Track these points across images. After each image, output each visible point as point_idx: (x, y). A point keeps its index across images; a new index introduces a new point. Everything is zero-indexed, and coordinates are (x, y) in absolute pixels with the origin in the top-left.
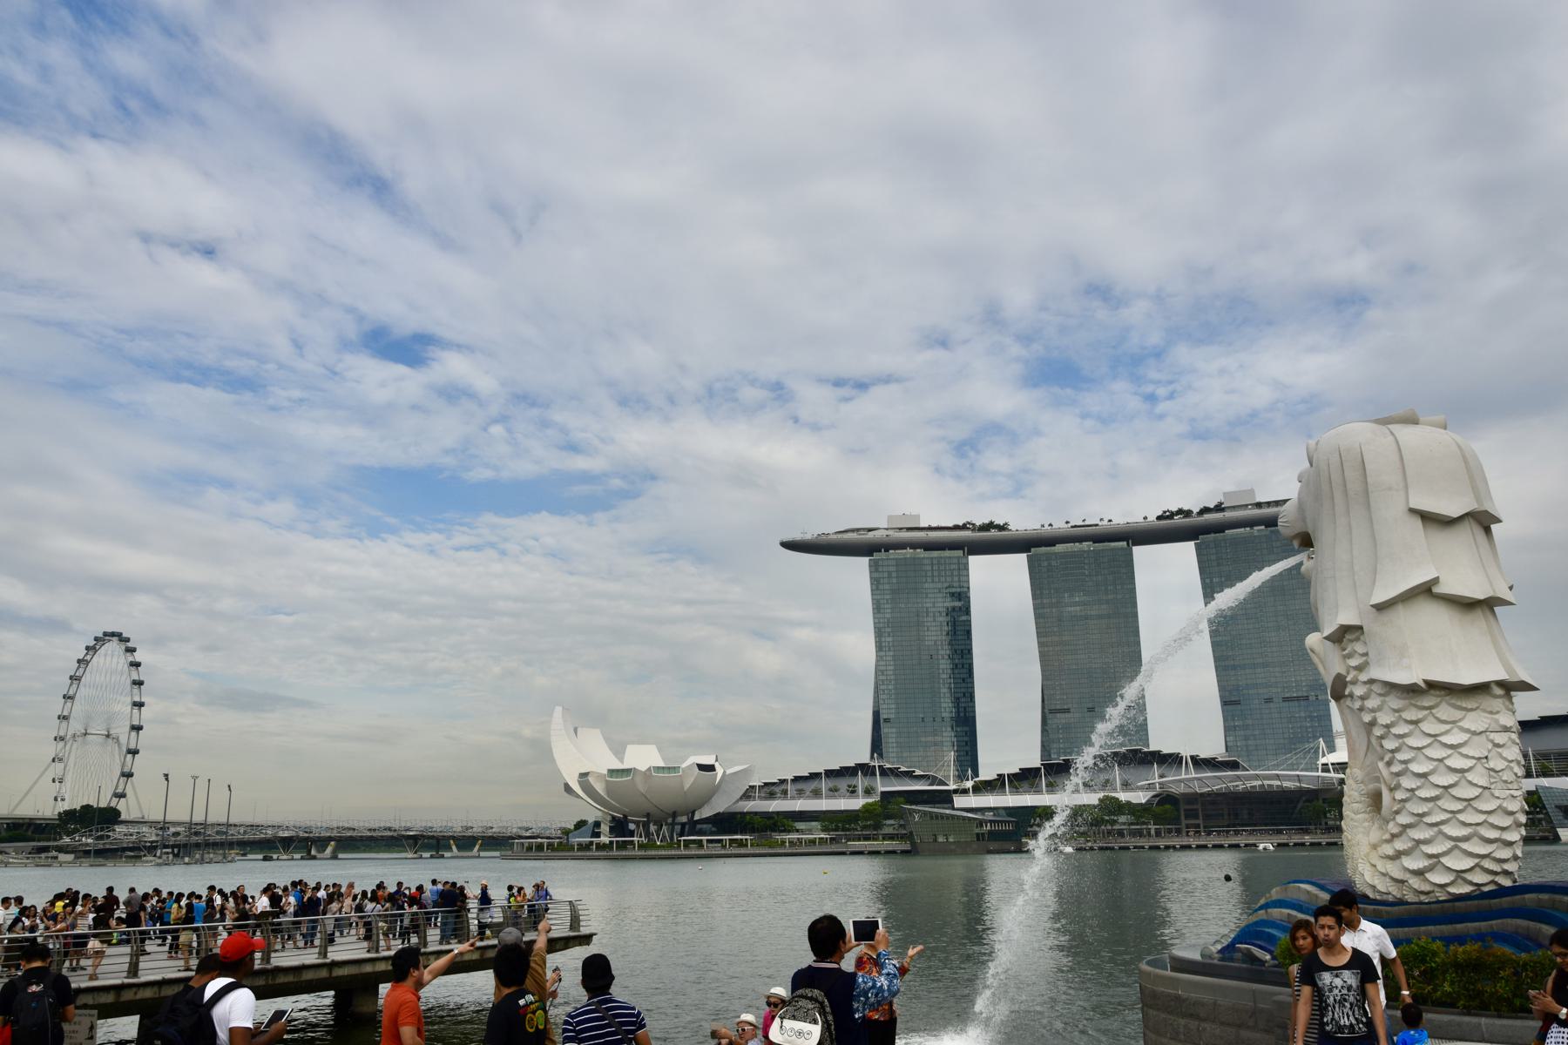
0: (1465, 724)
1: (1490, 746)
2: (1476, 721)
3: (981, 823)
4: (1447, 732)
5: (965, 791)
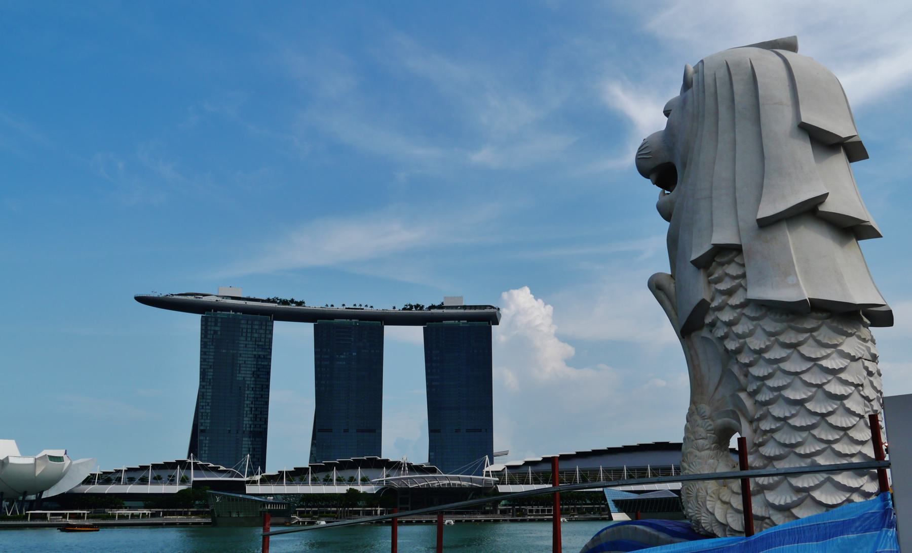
0: (845, 348)
1: (865, 373)
2: (851, 345)
3: (264, 504)
4: (827, 357)
5: (254, 482)
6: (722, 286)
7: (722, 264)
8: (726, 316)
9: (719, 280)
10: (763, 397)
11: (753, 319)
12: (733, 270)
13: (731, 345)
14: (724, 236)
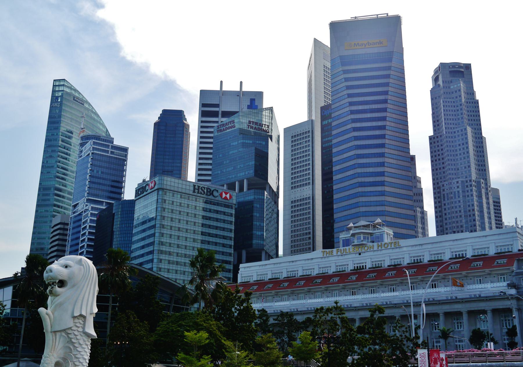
6: (78, 325)
7: (78, 319)
8: (76, 333)
9: (76, 323)
10: (78, 356)
11: (81, 336)
12: (81, 321)
13: (73, 340)
14: (84, 313)
